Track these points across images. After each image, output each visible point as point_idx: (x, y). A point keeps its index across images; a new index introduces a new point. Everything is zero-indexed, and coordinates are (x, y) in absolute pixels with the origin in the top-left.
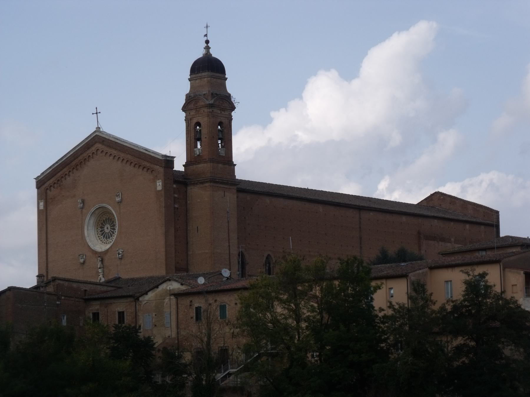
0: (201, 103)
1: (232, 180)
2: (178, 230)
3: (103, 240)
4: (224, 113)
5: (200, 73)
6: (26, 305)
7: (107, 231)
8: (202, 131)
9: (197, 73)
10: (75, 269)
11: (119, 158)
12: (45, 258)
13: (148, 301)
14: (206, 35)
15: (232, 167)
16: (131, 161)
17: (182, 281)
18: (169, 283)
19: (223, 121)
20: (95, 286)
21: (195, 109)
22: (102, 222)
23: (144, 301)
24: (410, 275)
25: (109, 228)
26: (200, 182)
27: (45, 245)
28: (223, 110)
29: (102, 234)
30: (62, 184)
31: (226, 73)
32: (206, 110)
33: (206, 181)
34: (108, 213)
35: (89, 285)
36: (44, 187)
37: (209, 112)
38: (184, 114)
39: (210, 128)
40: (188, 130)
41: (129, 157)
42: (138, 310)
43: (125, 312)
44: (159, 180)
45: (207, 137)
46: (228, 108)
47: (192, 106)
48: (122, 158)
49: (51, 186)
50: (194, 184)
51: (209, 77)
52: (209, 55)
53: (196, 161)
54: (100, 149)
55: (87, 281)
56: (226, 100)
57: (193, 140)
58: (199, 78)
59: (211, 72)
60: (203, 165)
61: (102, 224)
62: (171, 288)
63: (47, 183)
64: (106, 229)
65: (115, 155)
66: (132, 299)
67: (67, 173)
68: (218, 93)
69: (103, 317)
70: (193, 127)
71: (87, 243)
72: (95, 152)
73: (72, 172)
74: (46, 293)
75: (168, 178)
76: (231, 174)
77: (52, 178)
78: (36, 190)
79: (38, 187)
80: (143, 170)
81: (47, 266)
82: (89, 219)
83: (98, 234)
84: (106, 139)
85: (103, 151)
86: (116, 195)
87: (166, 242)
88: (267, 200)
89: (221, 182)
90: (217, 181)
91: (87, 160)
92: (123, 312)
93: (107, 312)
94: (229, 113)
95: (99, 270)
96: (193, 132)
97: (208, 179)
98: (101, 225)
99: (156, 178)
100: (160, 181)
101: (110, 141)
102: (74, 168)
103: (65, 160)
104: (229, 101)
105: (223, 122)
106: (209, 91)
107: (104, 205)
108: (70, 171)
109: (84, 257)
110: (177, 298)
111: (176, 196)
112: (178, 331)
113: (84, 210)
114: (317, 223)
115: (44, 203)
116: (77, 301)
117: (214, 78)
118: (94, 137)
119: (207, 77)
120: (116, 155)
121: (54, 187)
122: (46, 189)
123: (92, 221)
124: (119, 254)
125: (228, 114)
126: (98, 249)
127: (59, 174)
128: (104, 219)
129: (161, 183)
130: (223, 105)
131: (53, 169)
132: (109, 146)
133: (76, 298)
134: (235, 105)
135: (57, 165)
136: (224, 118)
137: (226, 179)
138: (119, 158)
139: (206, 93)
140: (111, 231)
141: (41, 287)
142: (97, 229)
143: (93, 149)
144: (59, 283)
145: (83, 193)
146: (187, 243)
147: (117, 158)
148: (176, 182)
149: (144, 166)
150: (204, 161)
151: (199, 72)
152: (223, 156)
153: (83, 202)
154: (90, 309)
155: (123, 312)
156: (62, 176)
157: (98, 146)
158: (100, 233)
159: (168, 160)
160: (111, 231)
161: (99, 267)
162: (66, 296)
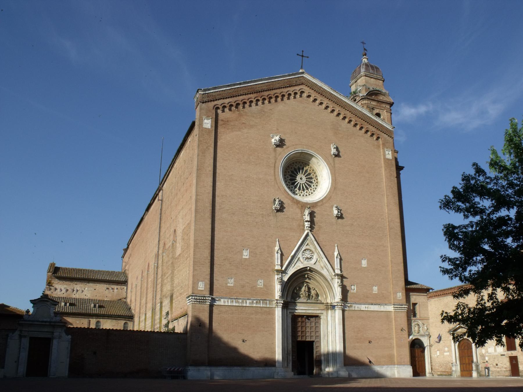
64: (299, 179)
115: (211, 121)
131: (231, 89)
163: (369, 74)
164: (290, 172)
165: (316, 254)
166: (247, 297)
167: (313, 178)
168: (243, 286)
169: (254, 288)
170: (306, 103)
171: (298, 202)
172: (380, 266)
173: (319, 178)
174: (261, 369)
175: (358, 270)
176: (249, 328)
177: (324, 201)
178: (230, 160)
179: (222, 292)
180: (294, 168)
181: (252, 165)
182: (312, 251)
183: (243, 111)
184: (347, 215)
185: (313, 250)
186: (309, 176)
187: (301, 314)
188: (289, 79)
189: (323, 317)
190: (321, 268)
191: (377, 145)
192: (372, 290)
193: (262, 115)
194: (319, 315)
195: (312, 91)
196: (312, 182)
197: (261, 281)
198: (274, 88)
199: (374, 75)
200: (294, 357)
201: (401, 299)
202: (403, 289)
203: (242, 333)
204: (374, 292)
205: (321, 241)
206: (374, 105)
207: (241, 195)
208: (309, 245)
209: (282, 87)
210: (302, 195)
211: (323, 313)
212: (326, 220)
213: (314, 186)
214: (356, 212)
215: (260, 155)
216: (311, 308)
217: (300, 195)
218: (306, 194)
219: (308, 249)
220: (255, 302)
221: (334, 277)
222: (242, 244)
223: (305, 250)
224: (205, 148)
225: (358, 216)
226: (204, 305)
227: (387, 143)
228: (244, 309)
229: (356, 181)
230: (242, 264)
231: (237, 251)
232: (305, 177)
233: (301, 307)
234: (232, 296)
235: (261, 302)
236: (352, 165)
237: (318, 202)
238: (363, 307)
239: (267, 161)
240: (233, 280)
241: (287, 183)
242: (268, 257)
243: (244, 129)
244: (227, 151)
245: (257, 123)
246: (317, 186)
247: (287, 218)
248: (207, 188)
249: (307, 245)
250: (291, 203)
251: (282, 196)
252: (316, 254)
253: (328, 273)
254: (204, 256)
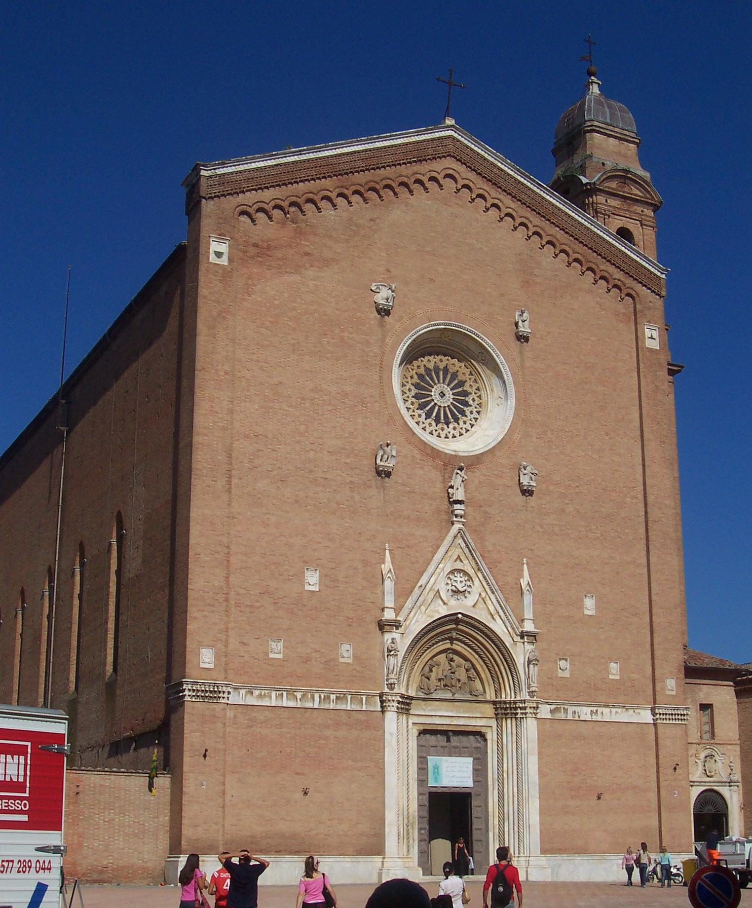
10: (351, 482)
29: (421, 407)
63: (248, 194)
71: (403, 418)
107: (467, 328)
128: (431, 366)
143: (439, 167)
163: (604, 126)
164: (415, 376)
165: (476, 581)
166: (315, 687)
167: (471, 393)
168: (307, 660)
169: (332, 663)
170: (457, 204)
171: (434, 454)
172: (626, 614)
173: (483, 393)
174: (349, 860)
175: (575, 623)
176: (320, 762)
177: (498, 454)
178: (274, 347)
179: (256, 673)
180: (425, 366)
181: (326, 358)
182: (469, 576)
183: (306, 221)
184: (551, 488)
185: (471, 572)
186: (460, 389)
187: (439, 728)
188: (418, 142)
189: (491, 736)
190: (489, 617)
191: (624, 314)
192: (607, 671)
193: (351, 233)
194: (483, 730)
195: (472, 176)
196: (467, 404)
197: (347, 647)
198: (380, 166)
199: (617, 130)
200: (423, 832)
201: (674, 693)
202: (679, 670)
203: (303, 774)
204: (611, 677)
205: (489, 551)
206: (614, 207)
207: (301, 434)
208: (461, 561)
209: (401, 162)
210: (443, 435)
211: (491, 727)
212: (501, 498)
213: (471, 413)
214: (573, 480)
215: (346, 334)
216: (464, 712)
217: (439, 436)
218: (452, 432)
219: (459, 571)
220: (333, 697)
221: (518, 639)
222: (302, 557)
223: (452, 572)
224: (215, 314)
225: (577, 490)
226: (214, 706)
227: (649, 308)
228: (308, 714)
229: (574, 405)
230: (305, 606)
231: (291, 573)
232: (451, 390)
233: (440, 710)
234: (280, 683)
235: (349, 697)
238: (585, 713)
239: (364, 351)
240: (281, 645)
241: (408, 404)
242: (364, 588)
243: (306, 269)
244: (267, 324)
245: (339, 253)
246: (478, 412)
247: (409, 492)
248: (221, 416)
249: (456, 561)
250: (419, 456)
251: (399, 439)
252: (476, 581)
253: (505, 630)
254: (213, 585)
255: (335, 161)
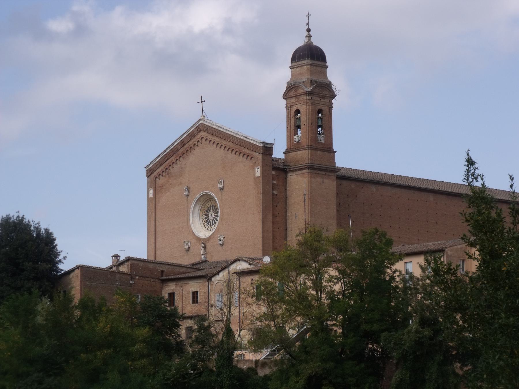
0: (300, 91)
1: (331, 167)
2: (276, 217)
3: (208, 227)
4: (324, 101)
5: (300, 61)
6: (95, 284)
7: (211, 218)
8: (301, 118)
9: (297, 62)
11: (222, 145)
12: (154, 245)
13: (219, 281)
14: (307, 24)
15: (332, 154)
16: (232, 149)
17: (251, 261)
18: (238, 263)
19: (323, 108)
20: (173, 267)
21: (295, 96)
22: (207, 209)
23: (216, 281)
24: (446, 250)
25: (213, 215)
26: (299, 169)
27: (154, 233)
28: (323, 98)
30: (170, 172)
31: (327, 61)
32: (305, 97)
33: (304, 167)
34: (212, 200)
35: (167, 266)
36: (153, 175)
37: (308, 99)
38: (284, 102)
39: (308, 116)
40: (288, 118)
41: (231, 144)
42: (210, 290)
43: (198, 293)
44: (257, 166)
45: (306, 125)
46: (328, 96)
47: (292, 93)
48: (224, 146)
49: (160, 174)
50: (293, 171)
51: (309, 65)
52: (310, 43)
53: (296, 148)
54: (204, 137)
55: (165, 262)
56: (326, 87)
57: (293, 127)
58: (299, 66)
59: (311, 59)
60: (301, 152)
61: (207, 211)
62: (240, 268)
63: (156, 171)
64: (210, 216)
65: (218, 142)
66: (205, 280)
67: (174, 161)
68: (317, 81)
69: (178, 297)
70: (293, 114)
72: (200, 140)
73: (179, 160)
74: (119, 272)
75: (267, 165)
76: (331, 161)
77: (161, 167)
78: (146, 179)
79: (148, 176)
80: (243, 157)
81: (155, 253)
82: (194, 207)
83: (203, 221)
84: (210, 127)
85: (207, 139)
86: (219, 182)
87: (263, 229)
88: (373, 188)
89: (319, 169)
90: (315, 167)
91: (193, 148)
92: (197, 292)
93: (182, 292)
94: (329, 101)
95: (203, 256)
96: (293, 120)
97: (305, 166)
98: (205, 213)
99: (255, 165)
100: (259, 167)
101: (213, 129)
102: (180, 157)
103: (172, 149)
104: (329, 88)
105: (323, 109)
106: (308, 79)
107: (208, 192)
108: (177, 160)
109: (189, 244)
110: (239, 277)
111: (275, 182)
112: (240, 309)
113: (189, 198)
114: (427, 212)
115: (153, 191)
116: (153, 282)
117: (314, 66)
118: (199, 125)
119: (307, 65)
120: (219, 143)
121: (162, 176)
122: (155, 177)
123: (197, 209)
124: (220, 241)
125: (328, 101)
126: (202, 236)
127: (167, 162)
129: (259, 170)
130: (323, 93)
132: (212, 134)
133: (151, 278)
134: (336, 93)
135: (165, 153)
136: (324, 106)
137: (325, 166)
138: (222, 145)
139: (305, 81)
140: (215, 218)
141: (113, 267)
142: (202, 216)
143: (198, 137)
144: (133, 263)
145: (189, 181)
146: (286, 229)
147: (219, 145)
148: (275, 169)
149: (244, 153)
150: (302, 148)
151: (299, 60)
152: (322, 144)
153: (188, 189)
154: (167, 289)
155: (197, 292)
156: (170, 164)
157: (202, 134)
158: (205, 220)
159: (267, 147)
160: (215, 218)
161: (202, 253)
162: (141, 276)
225: (236, 239)
236: (233, 193)
237: (211, 235)
255: (173, 150)
